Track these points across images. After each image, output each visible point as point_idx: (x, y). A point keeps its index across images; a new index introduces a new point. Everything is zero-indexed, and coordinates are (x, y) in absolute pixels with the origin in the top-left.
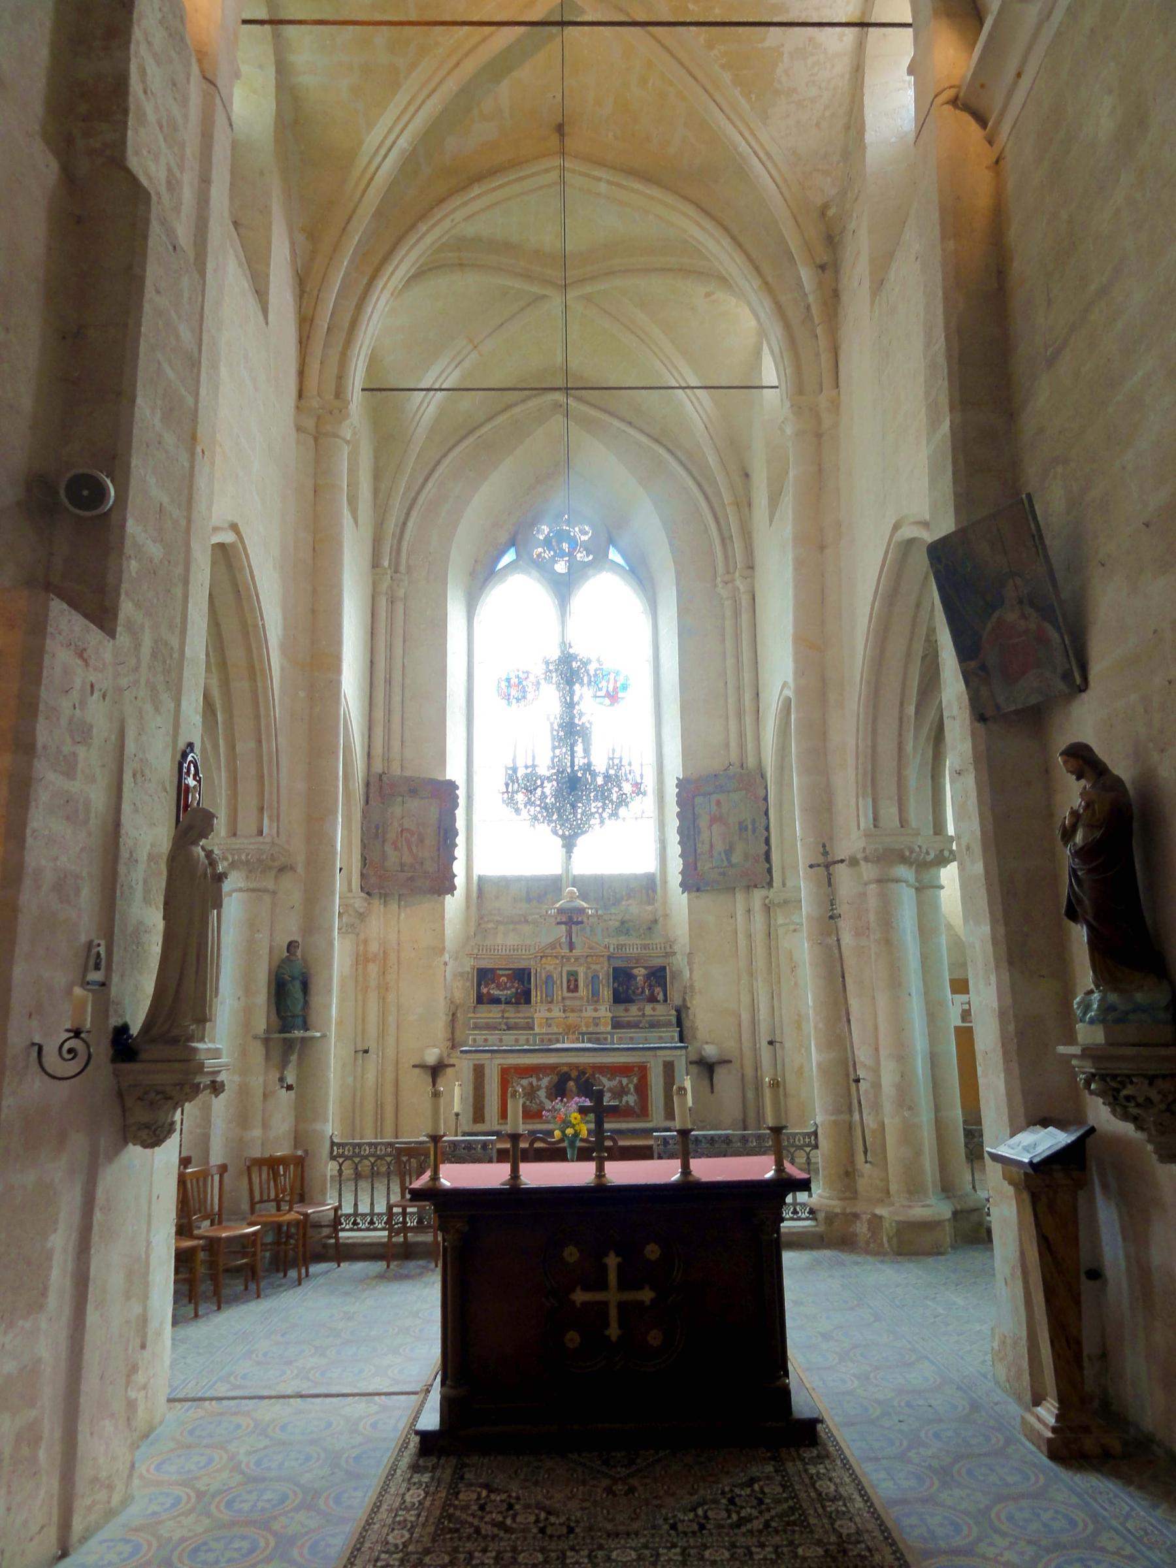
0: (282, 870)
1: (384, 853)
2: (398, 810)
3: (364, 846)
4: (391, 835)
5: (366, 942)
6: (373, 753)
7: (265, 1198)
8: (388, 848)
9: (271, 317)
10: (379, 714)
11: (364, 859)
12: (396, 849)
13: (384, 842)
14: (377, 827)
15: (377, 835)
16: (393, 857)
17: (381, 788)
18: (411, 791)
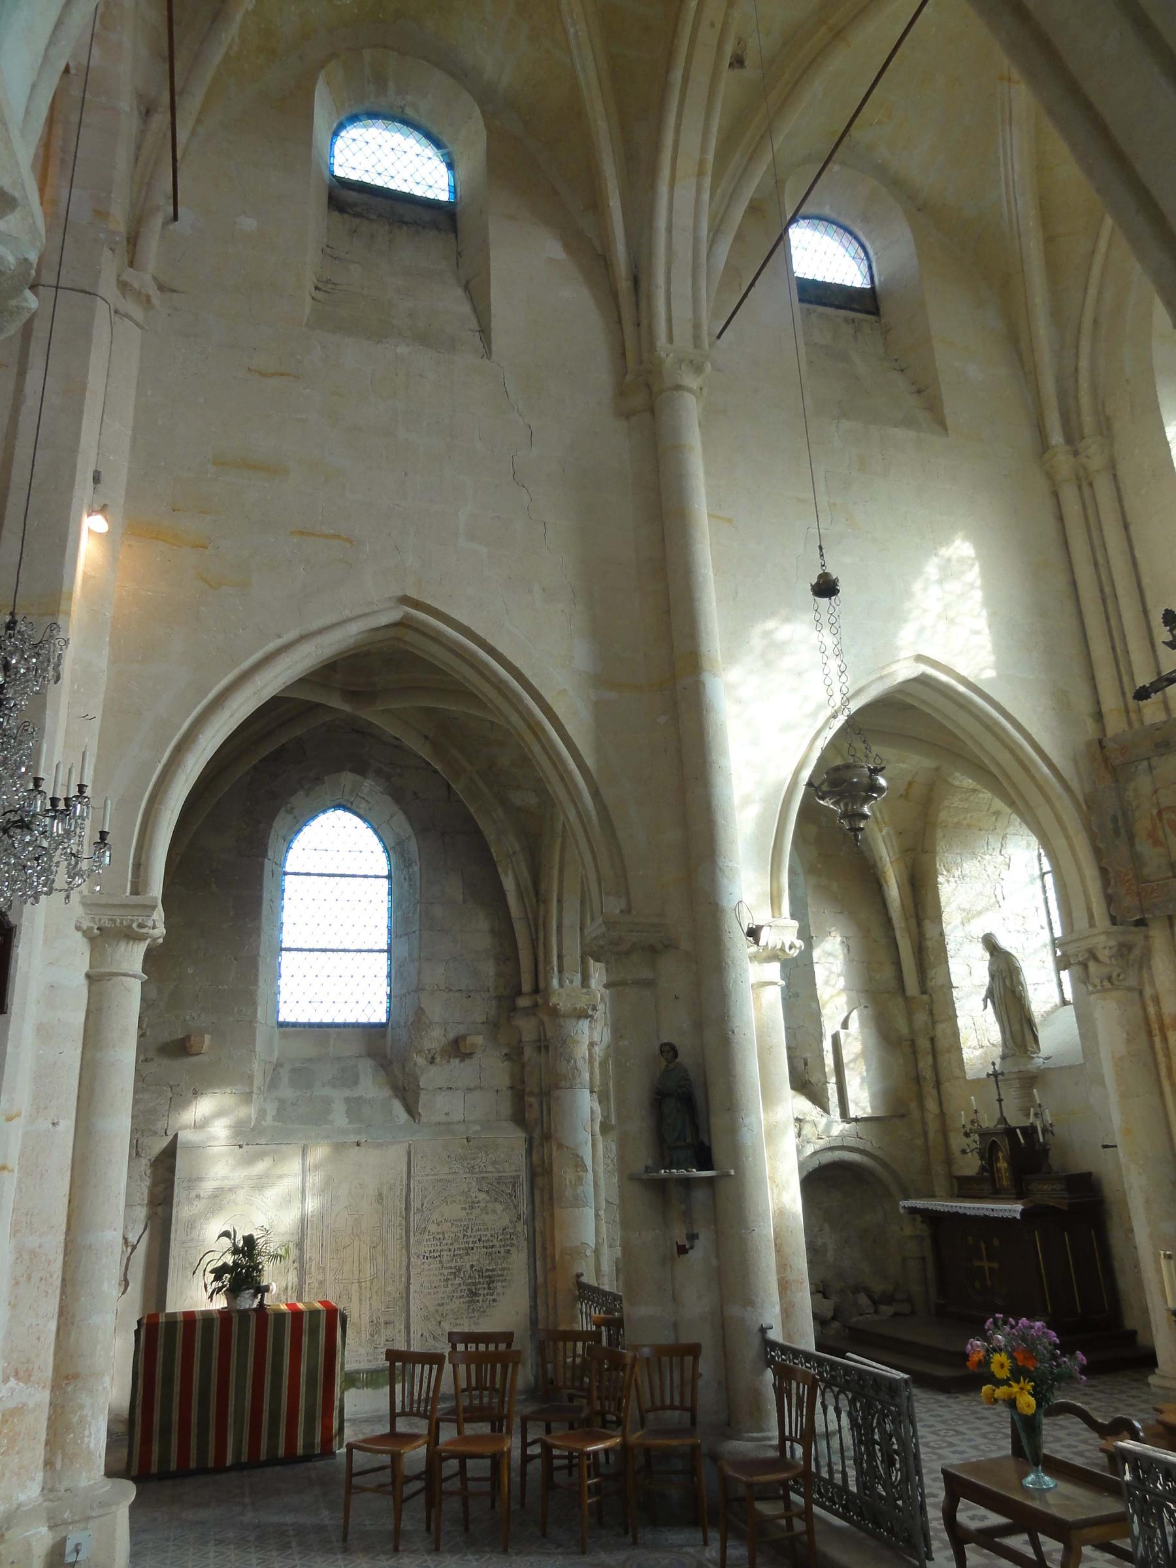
0: (653, 952)
1: (1137, 859)
2: (1143, 783)
3: (1098, 853)
4: (1143, 825)
5: (1157, 1000)
6: (1105, 709)
7: (668, 1402)
8: (1144, 847)
9: (499, 341)
10: (1100, 650)
11: (1104, 872)
12: (1156, 843)
13: (1131, 838)
14: (1115, 819)
15: (1117, 832)
16: (1153, 858)
17: (1106, 760)
18: (1157, 746)
